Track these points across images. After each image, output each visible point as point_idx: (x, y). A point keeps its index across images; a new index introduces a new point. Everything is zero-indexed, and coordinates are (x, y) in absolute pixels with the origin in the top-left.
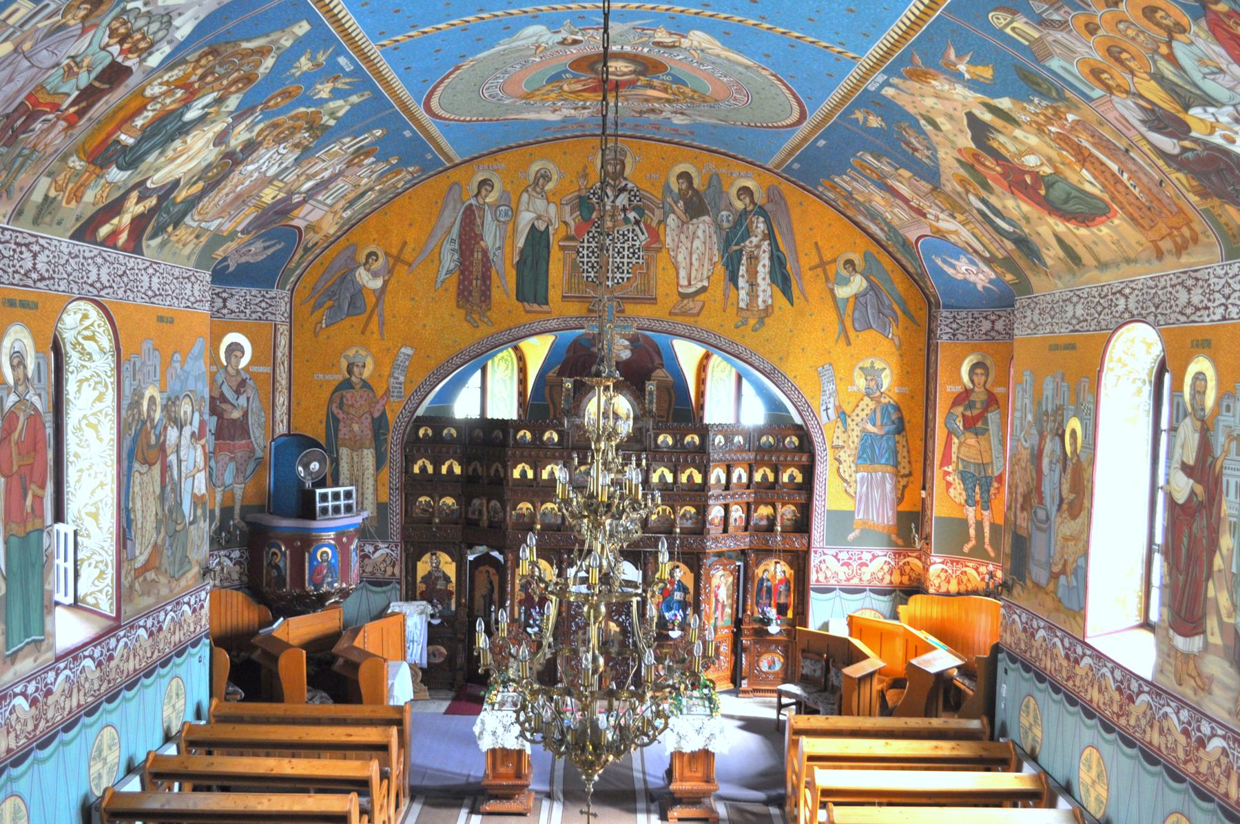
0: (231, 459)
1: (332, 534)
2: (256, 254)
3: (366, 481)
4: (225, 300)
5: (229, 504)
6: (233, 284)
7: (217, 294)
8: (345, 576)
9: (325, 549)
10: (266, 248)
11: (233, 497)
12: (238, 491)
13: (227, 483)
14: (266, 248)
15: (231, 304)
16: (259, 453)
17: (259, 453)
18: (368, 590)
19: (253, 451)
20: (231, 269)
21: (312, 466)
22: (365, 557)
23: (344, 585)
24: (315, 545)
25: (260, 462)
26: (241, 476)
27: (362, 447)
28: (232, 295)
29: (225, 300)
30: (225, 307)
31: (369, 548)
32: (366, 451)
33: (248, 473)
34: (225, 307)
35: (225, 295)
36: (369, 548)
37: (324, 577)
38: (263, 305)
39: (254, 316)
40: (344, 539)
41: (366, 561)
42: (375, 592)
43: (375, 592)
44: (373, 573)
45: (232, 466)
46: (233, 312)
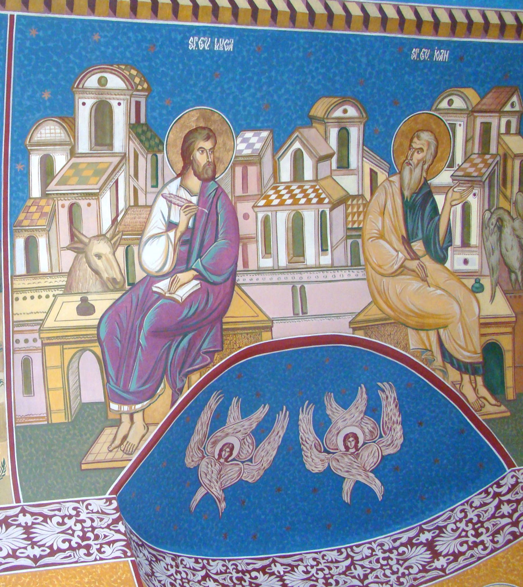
2: (375, 437)
4: (430, 545)
6: (431, 511)
7: (410, 543)
10: (373, 410)
14: (373, 410)
15: (447, 544)
20: (377, 487)
28: (441, 529)
29: (430, 545)
30: (436, 555)
34: (436, 555)
35: (424, 537)
38: (506, 509)
39: (500, 538)
46: (456, 556)
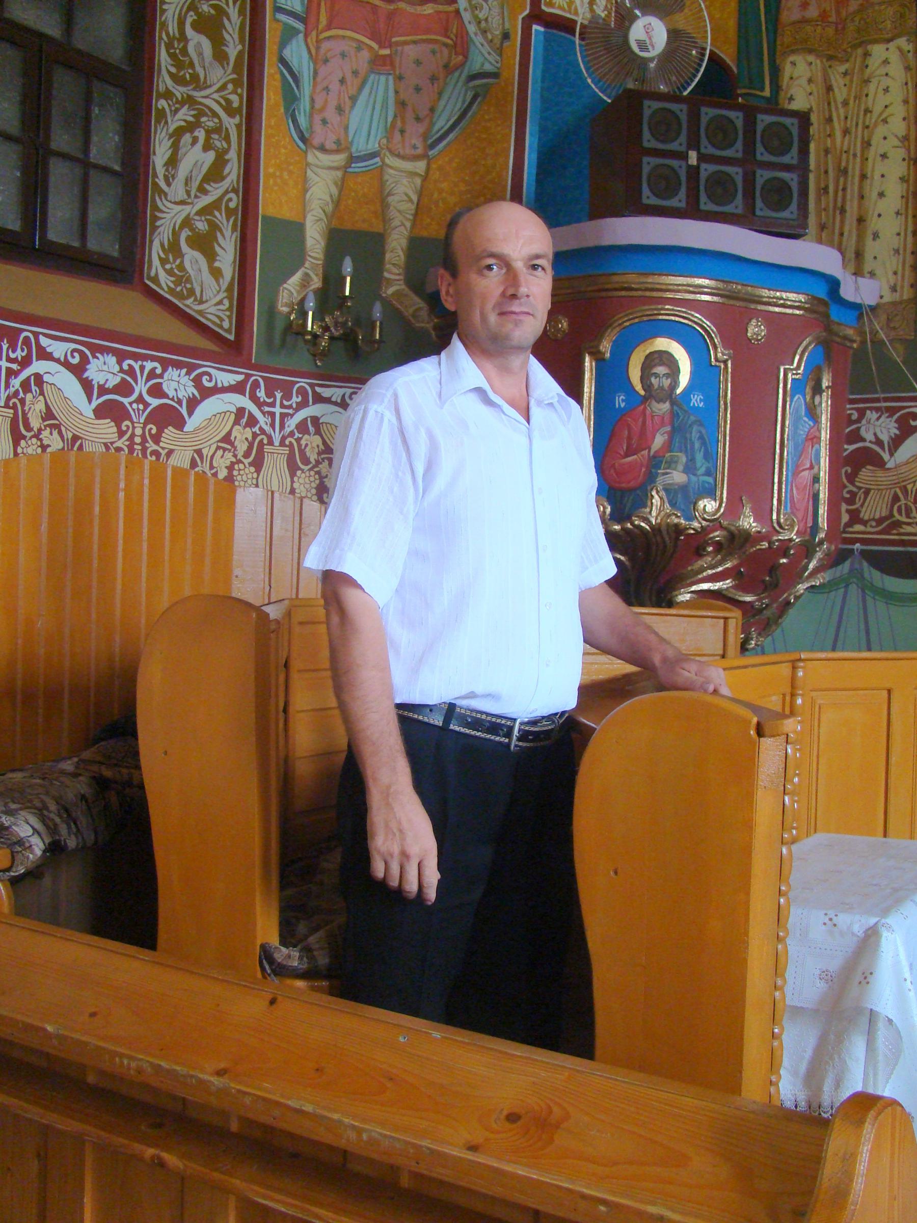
0: (379, 64)
1: (703, 286)
3: (877, 168)
5: (362, 219)
8: (750, 473)
9: (663, 344)
11: (382, 199)
12: (403, 181)
13: (361, 145)
16: (482, 57)
17: (482, 57)
18: (866, 587)
19: (462, 45)
21: (637, 32)
22: (854, 459)
23: (748, 522)
24: (625, 320)
25: (483, 86)
26: (415, 132)
27: (863, 42)
31: (878, 427)
32: (878, 51)
33: (442, 123)
36: (878, 427)
37: (655, 463)
40: (756, 330)
41: (866, 475)
42: (889, 597)
43: (889, 597)
44: (890, 524)
45: (382, 87)
